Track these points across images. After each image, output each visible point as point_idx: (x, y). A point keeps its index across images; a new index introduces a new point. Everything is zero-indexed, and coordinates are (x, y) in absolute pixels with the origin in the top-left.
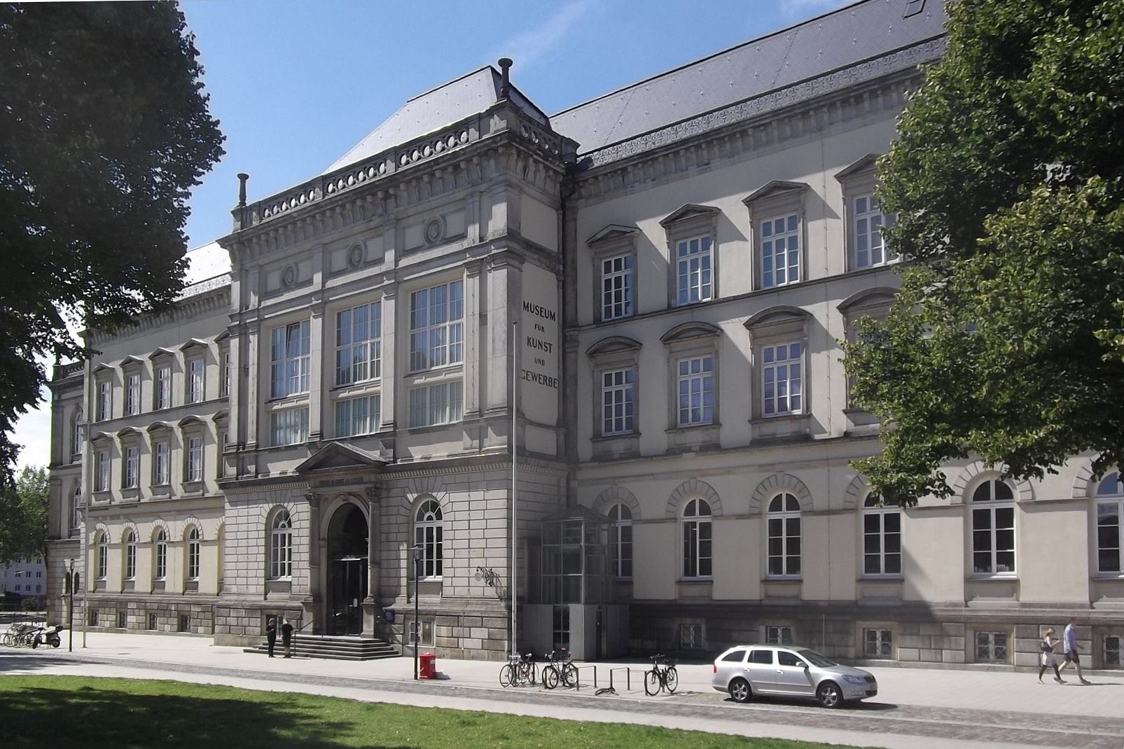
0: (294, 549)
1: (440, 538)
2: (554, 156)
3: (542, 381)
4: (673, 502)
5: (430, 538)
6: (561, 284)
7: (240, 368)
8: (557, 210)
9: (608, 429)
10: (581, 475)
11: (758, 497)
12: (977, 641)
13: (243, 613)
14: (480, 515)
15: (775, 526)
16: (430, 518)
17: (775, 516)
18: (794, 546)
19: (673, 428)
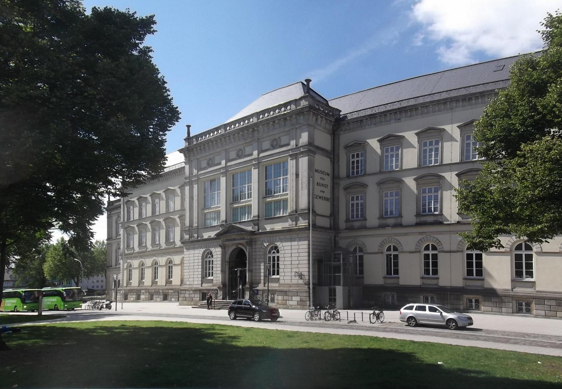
0: (214, 266)
1: (278, 260)
2: (330, 115)
3: (323, 199)
4: (382, 245)
5: (274, 260)
6: (332, 162)
7: (190, 197)
8: (331, 135)
9: (353, 217)
10: (340, 235)
11: (419, 245)
12: (517, 305)
13: (192, 292)
14: (296, 251)
15: (427, 257)
16: (274, 253)
17: (427, 252)
18: (435, 264)
19: (381, 217)
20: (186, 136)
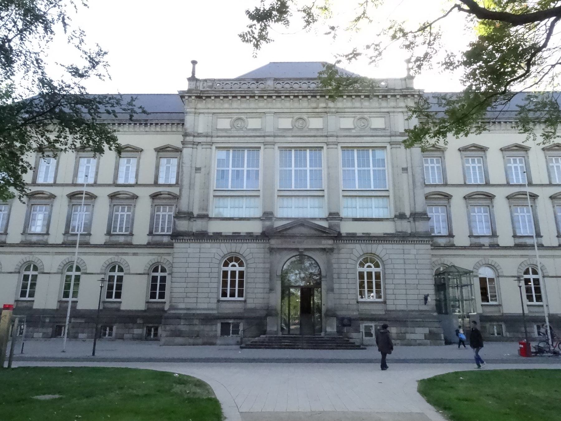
20: (190, 75)
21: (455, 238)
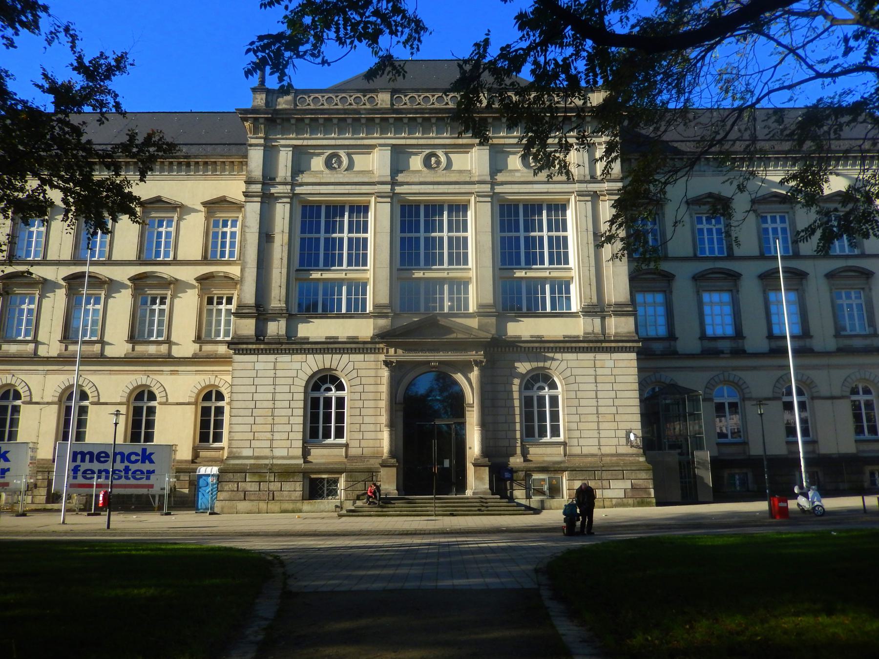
21: (678, 342)
